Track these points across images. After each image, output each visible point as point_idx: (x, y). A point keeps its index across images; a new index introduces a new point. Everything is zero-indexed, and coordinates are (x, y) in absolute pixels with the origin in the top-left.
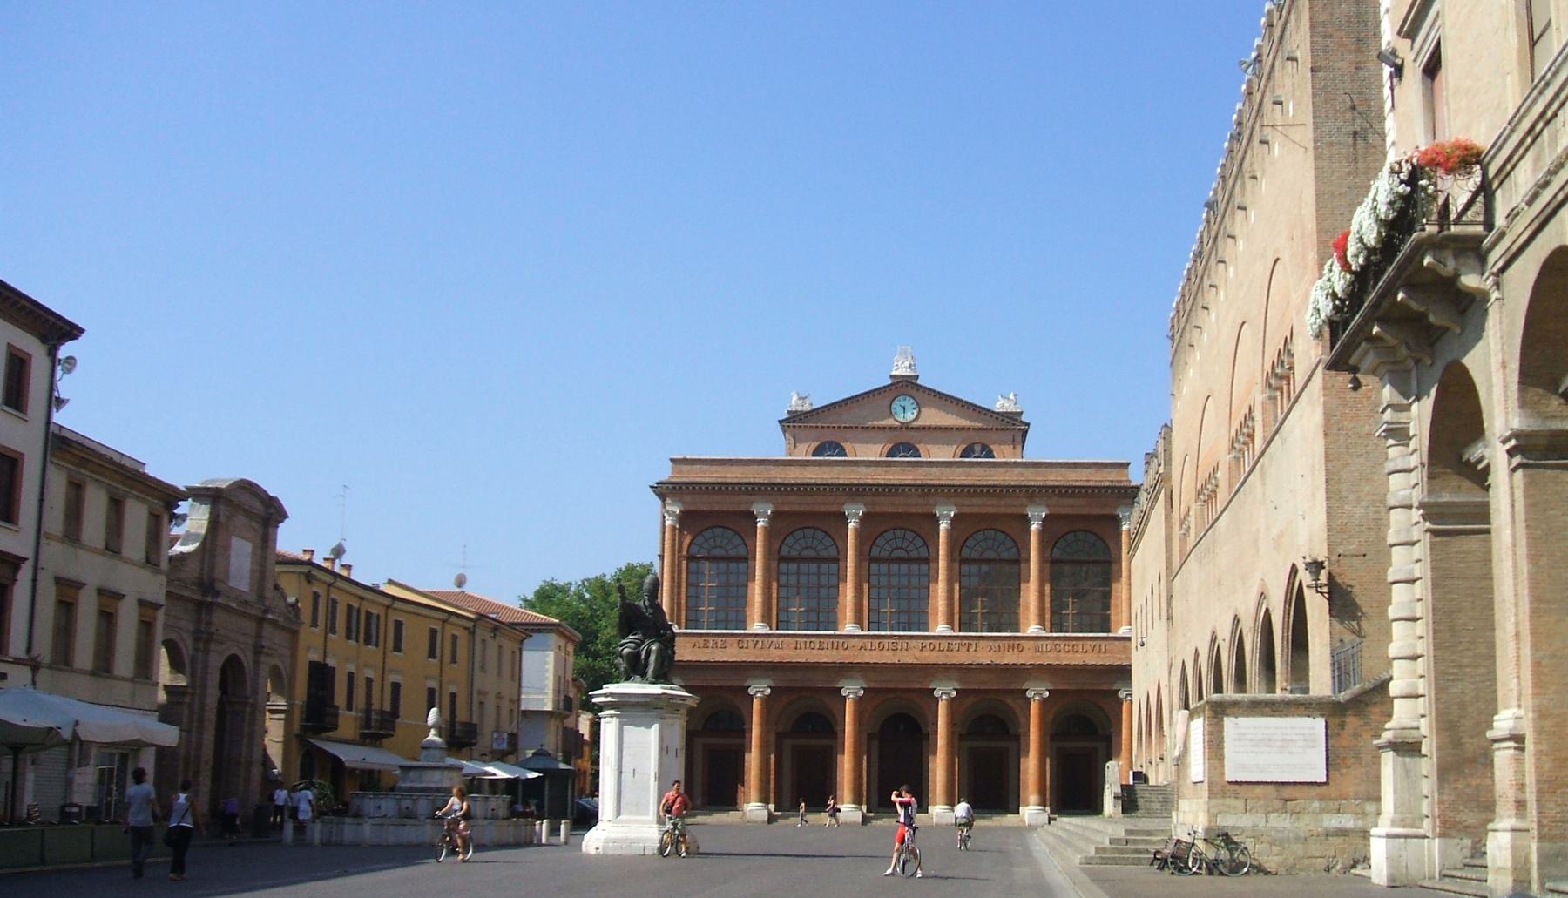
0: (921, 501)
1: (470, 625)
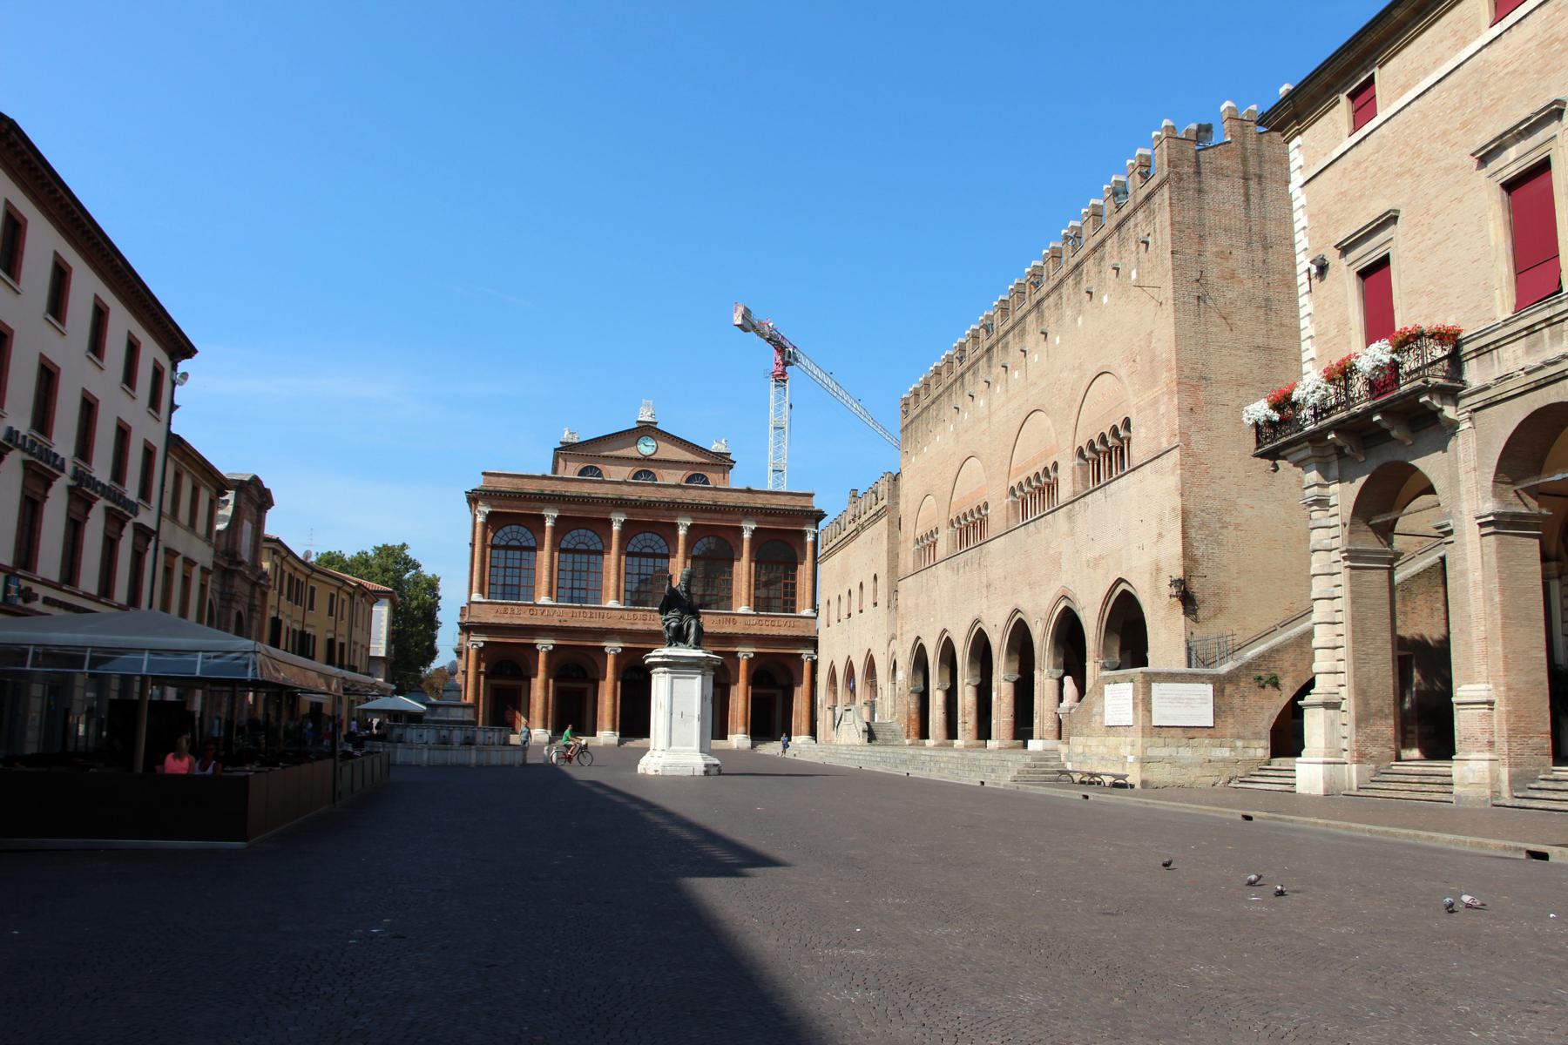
1: (351, 591)
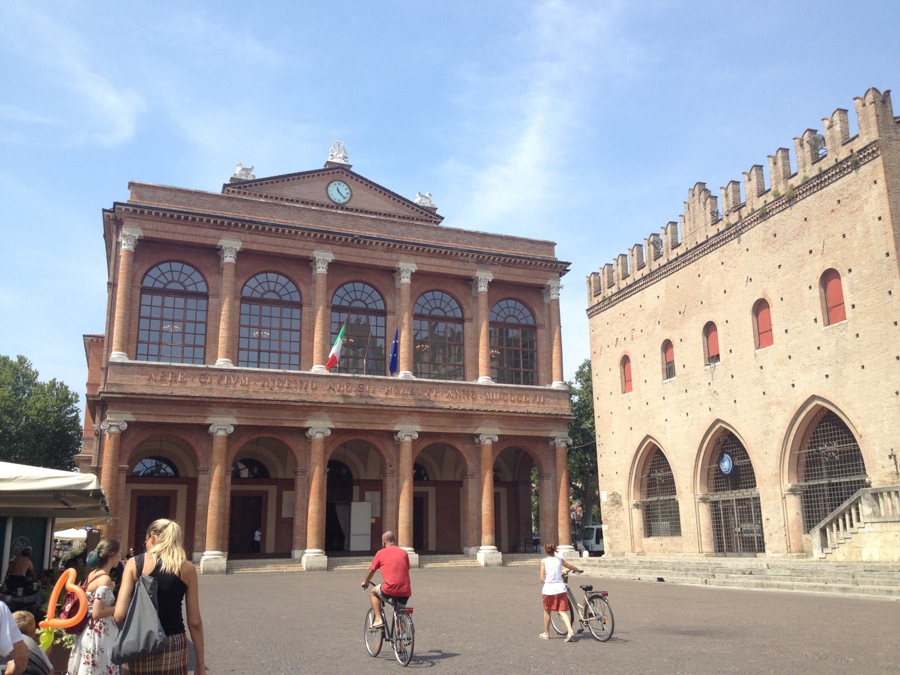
0: (385, 255)
